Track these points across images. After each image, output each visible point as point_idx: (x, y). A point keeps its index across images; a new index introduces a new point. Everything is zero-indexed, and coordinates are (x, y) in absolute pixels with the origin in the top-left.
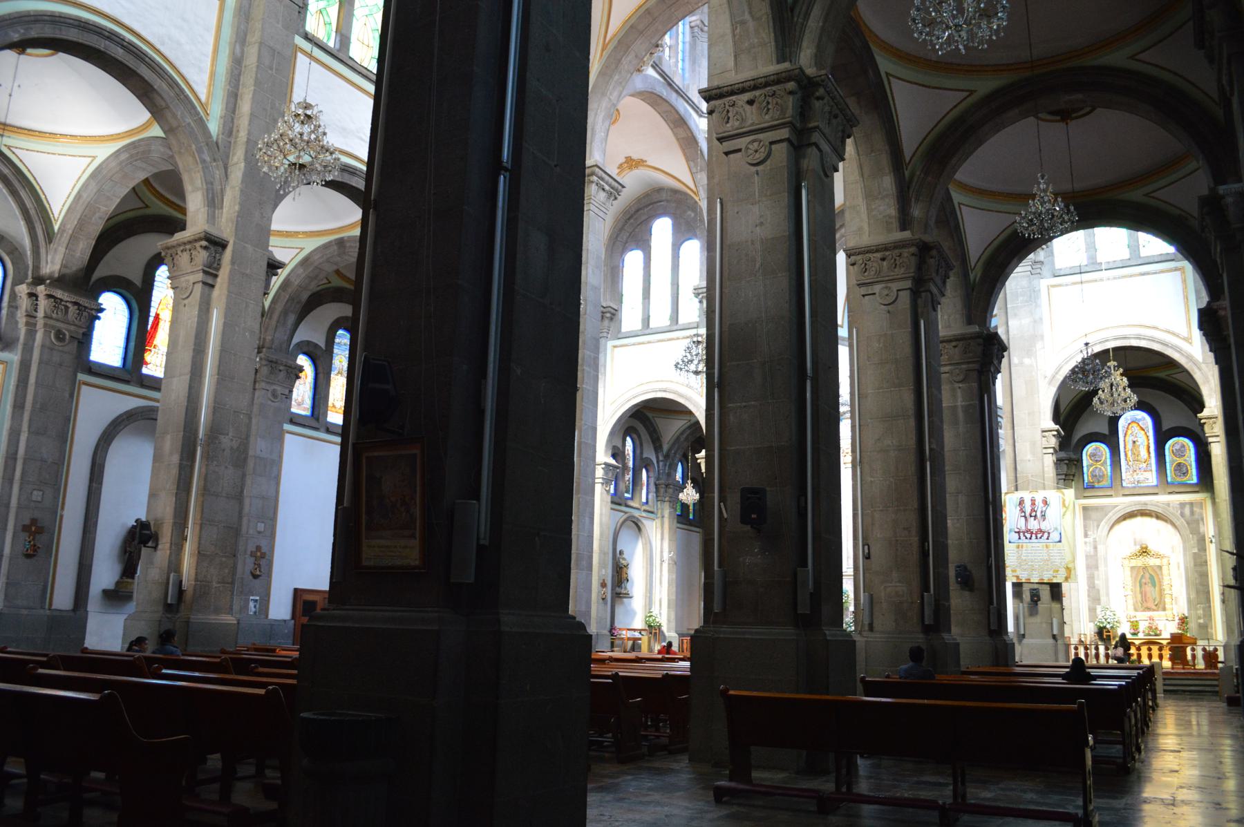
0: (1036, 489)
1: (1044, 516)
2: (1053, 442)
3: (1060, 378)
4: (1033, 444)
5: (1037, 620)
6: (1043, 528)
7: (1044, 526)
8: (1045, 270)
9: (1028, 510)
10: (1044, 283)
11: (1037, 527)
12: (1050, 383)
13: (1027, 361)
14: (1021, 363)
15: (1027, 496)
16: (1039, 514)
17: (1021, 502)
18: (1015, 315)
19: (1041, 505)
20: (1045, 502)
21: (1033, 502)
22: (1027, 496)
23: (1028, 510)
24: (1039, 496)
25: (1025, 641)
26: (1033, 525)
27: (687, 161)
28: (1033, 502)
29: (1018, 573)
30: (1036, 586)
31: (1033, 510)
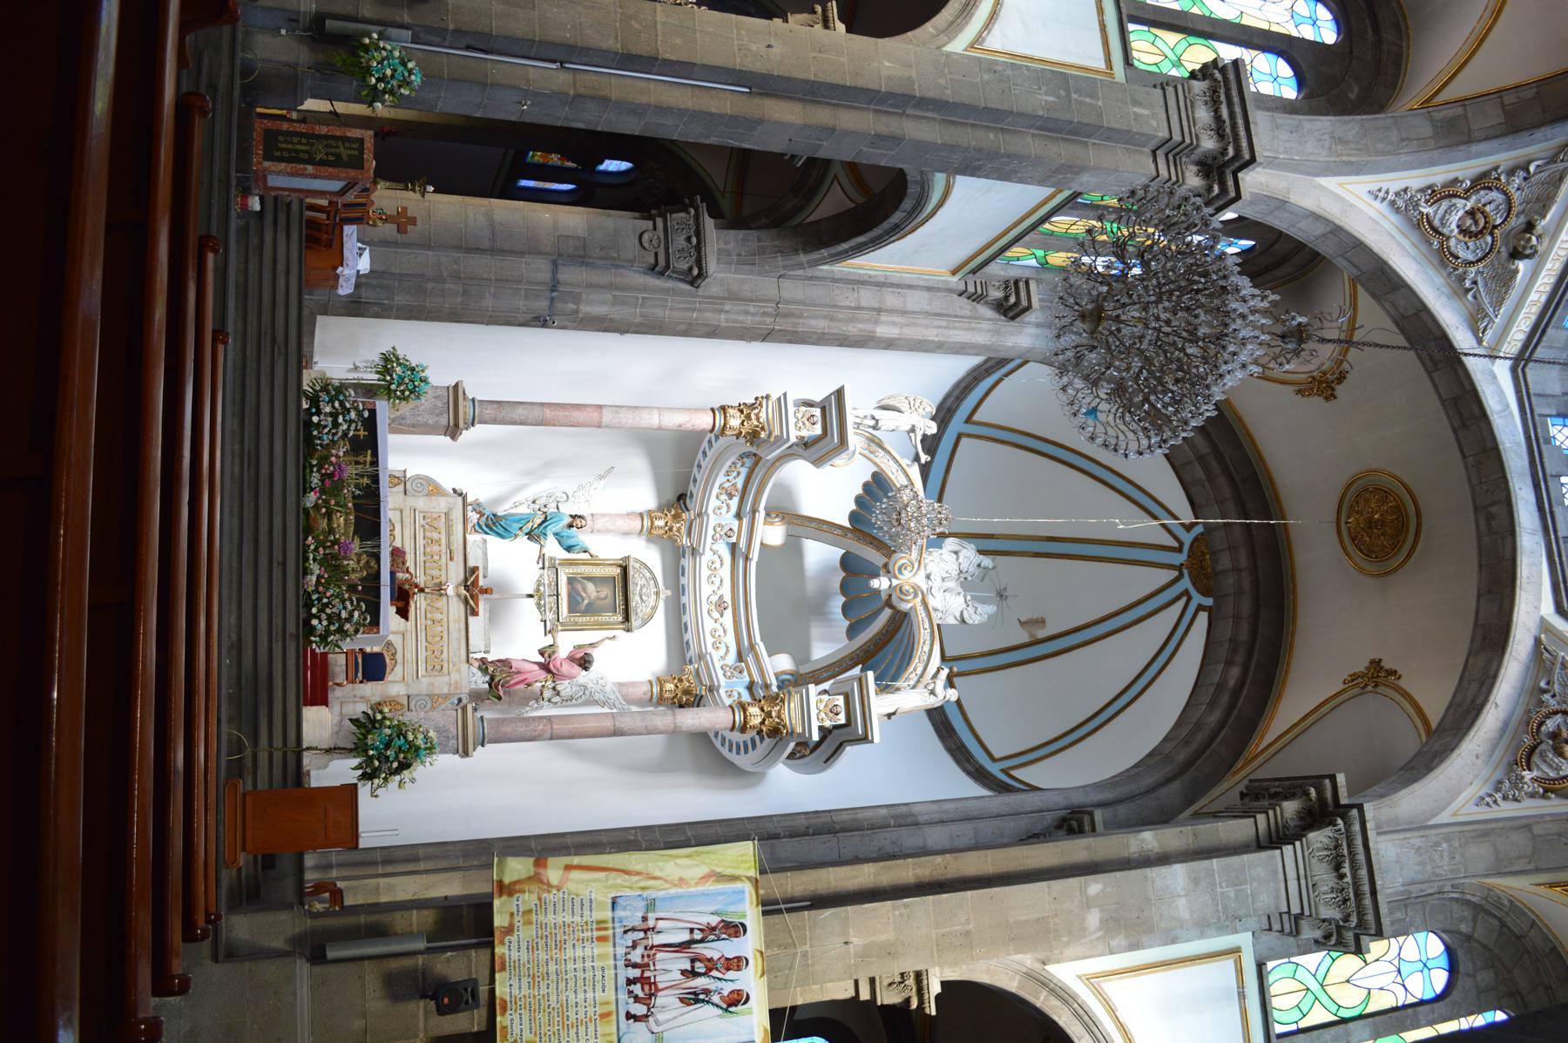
0: (770, 971)
1: (694, 998)
2: (889, 998)
3: (1043, 1001)
4: (889, 951)
5: (376, 1003)
6: (660, 1000)
7: (667, 1001)
8: (1272, 939)
9: (713, 950)
10: (1244, 940)
11: (662, 980)
12: (1030, 976)
13: (1093, 919)
14: (1087, 904)
15: (749, 945)
16: (700, 982)
17: (735, 929)
18: (1196, 881)
19: (727, 988)
20: (736, 1000)
21: (736, 963)
22: (749, 945)
23: (713, 950)
24: (750, 980)
25: (303, 968)
26: (670, 968)
27: (1540, 83)
28: (736, 963)
29: (524, 933)
30: (483, 989)
31: (711, 965)
